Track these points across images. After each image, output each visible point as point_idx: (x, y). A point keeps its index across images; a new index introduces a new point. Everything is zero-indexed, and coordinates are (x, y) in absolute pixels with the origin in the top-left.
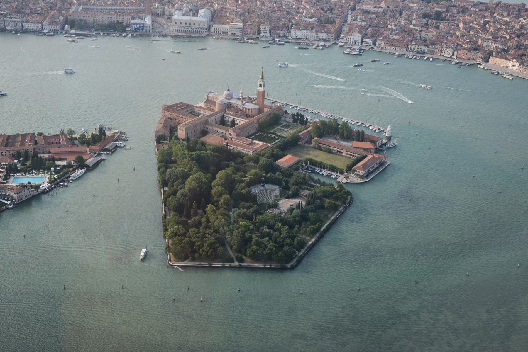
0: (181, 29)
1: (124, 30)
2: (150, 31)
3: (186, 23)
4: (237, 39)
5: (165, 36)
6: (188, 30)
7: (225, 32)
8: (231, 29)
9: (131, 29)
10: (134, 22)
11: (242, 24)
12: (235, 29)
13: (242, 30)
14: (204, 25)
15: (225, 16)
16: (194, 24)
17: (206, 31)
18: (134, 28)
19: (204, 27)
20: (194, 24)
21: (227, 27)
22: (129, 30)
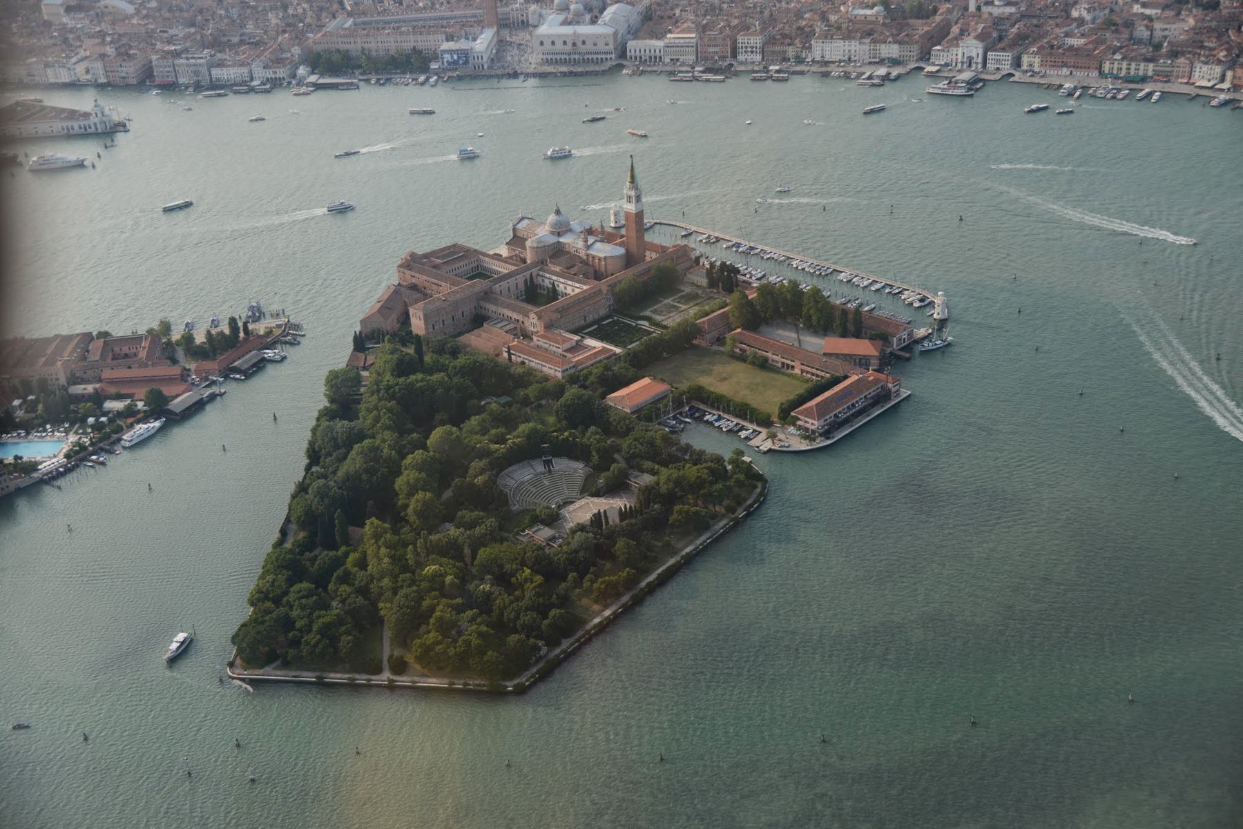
0: (554, 57)
1: (425, 69)
2: (483, 66)
3: (565, 43)
4: (680, 72)
5: (515, 75)
6: (570, 59)
7: (655, 57)
8: (669, 49)
9: (440, 63)
10: (447, 48)
11: (693, 35)
12: (677, 49)
13: (694, 49)
14: (607, 44)
15: (670, 17)
16: (584, 42)
17: (611, 59)
18: (447, 61)
19: (607, 47)
20: (584, 42)
21: (659, 44)
22: (437, 67)
